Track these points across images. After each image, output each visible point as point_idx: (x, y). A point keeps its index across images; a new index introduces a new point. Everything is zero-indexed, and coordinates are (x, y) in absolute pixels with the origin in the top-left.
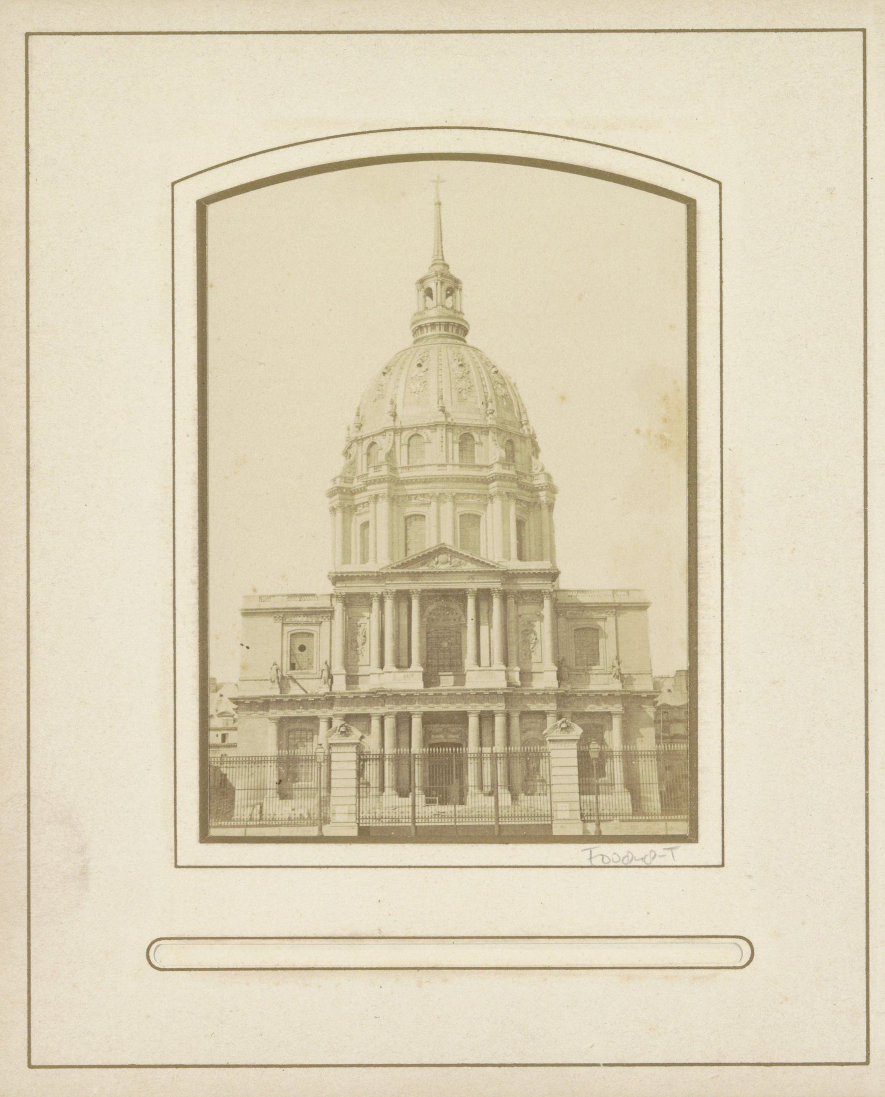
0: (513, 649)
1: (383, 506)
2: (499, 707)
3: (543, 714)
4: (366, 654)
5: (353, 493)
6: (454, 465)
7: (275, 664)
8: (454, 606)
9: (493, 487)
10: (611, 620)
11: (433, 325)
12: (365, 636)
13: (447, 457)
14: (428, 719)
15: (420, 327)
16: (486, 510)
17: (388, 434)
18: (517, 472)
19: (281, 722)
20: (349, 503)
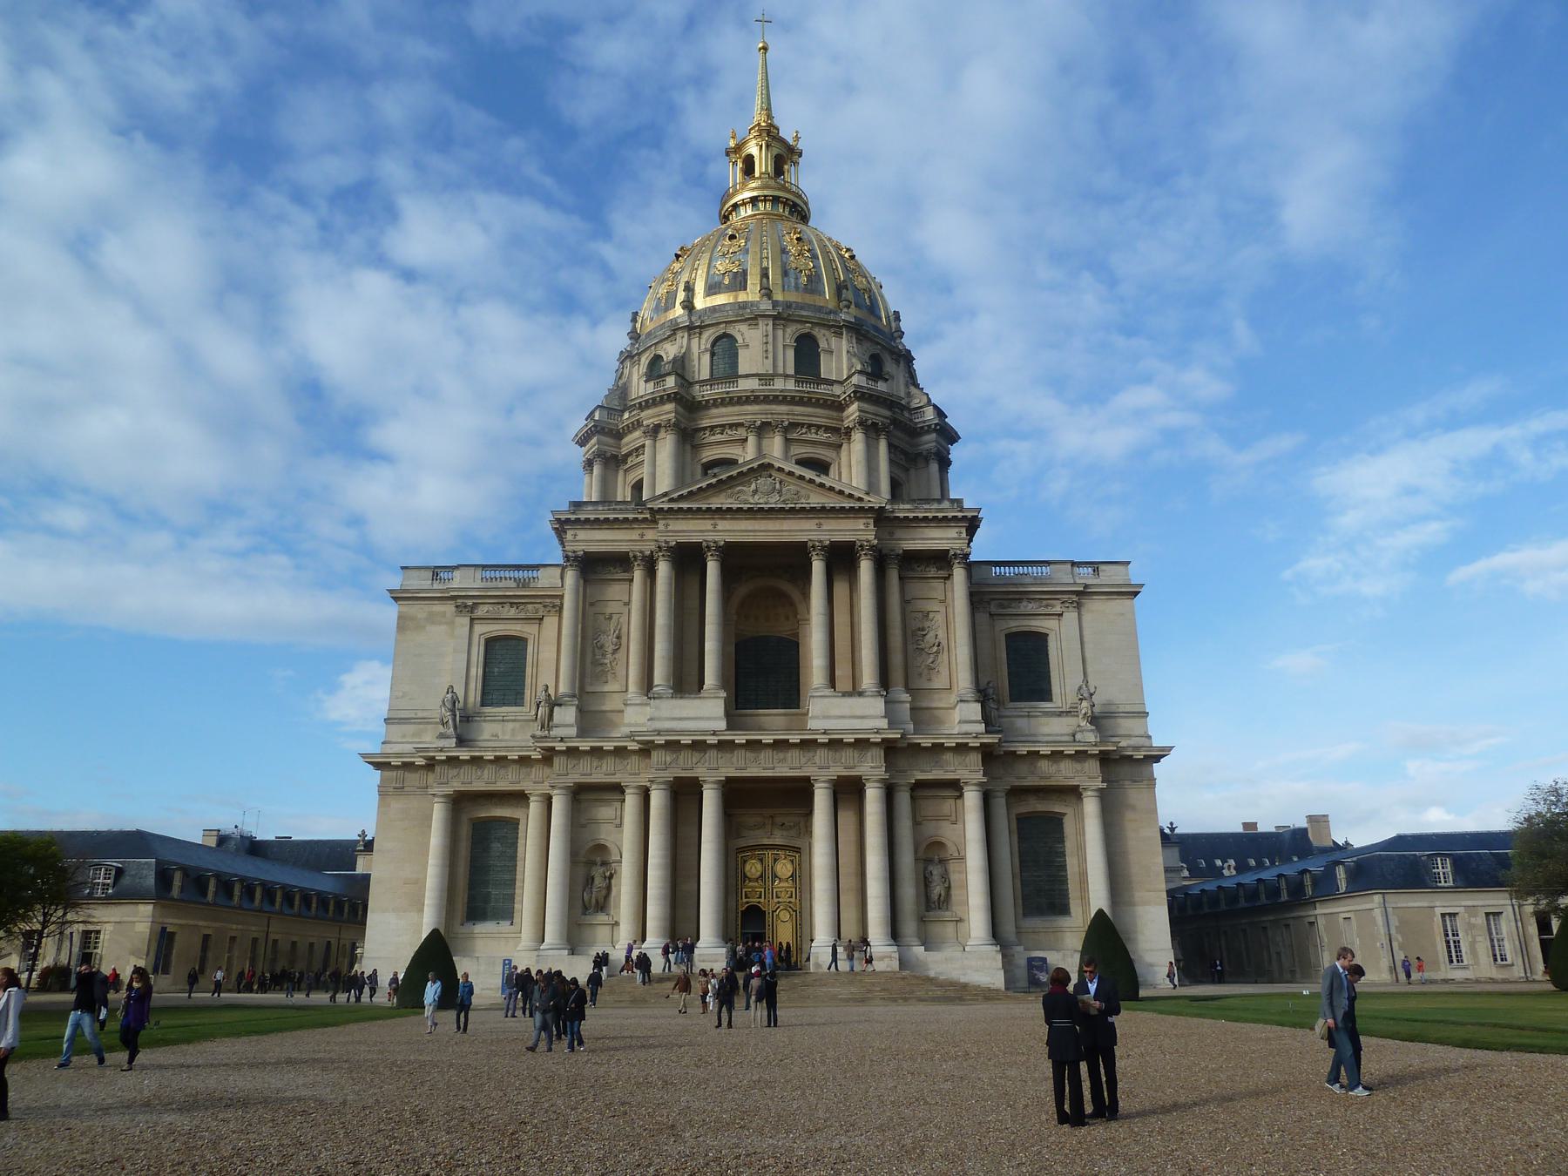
0: (896, 659)
1: (666, 446)
2: (871, 768)
3: (955, 787)
4: (621, 672)
5: (619, 435)
6: (786, 376)
7: (451, 689)
8: (786, 586)
9: (853, 411)
10: (1070, 616)
11: (754, 201)
12: (618, 637)
13: (775, 366)
14: (737, 794)
15: (735, 206)
16: (838, 454)
17: (679, 334)
19: (459, 802)
20: (614, 451)
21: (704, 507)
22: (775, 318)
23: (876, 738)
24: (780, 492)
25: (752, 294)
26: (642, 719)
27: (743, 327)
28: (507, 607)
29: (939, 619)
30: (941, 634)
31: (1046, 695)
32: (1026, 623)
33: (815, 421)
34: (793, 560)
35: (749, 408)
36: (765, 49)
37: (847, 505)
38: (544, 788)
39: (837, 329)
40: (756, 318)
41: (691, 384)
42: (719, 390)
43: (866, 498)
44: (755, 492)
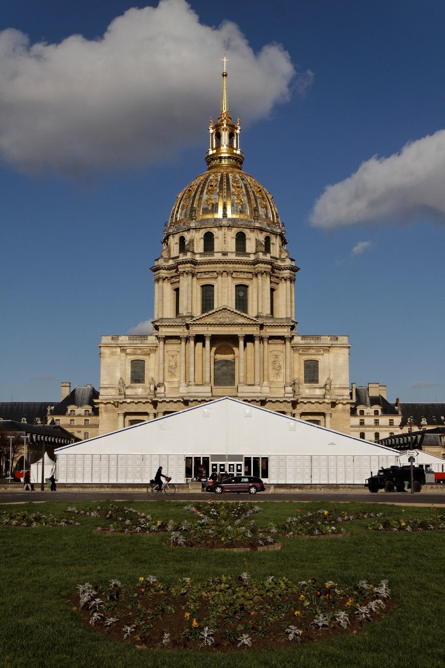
8: (230, 344)
11: (221, 158)
17: (191, 230)
18: (271, 257)
21: (205, 323)
22: (228, 227)
23: (258, 400)
24: (229, 318)
25: (219, 215)
26: (185, 391)
27: (216, 229)
28: (138, 350)
29: (281, 358)
30: (281, 363)
31: (317, 381)
32: (311, 357)
33: (243, 270)
34: (233, 340)
35: (218, 265)
36: (226, 76)
37: (251, 323)
38: (154, 411)
39: (253, 229)
40: (221, 227)
41: (196, 254)
42: (207, 258)
43: (257, 321)
44: (220, 318)
